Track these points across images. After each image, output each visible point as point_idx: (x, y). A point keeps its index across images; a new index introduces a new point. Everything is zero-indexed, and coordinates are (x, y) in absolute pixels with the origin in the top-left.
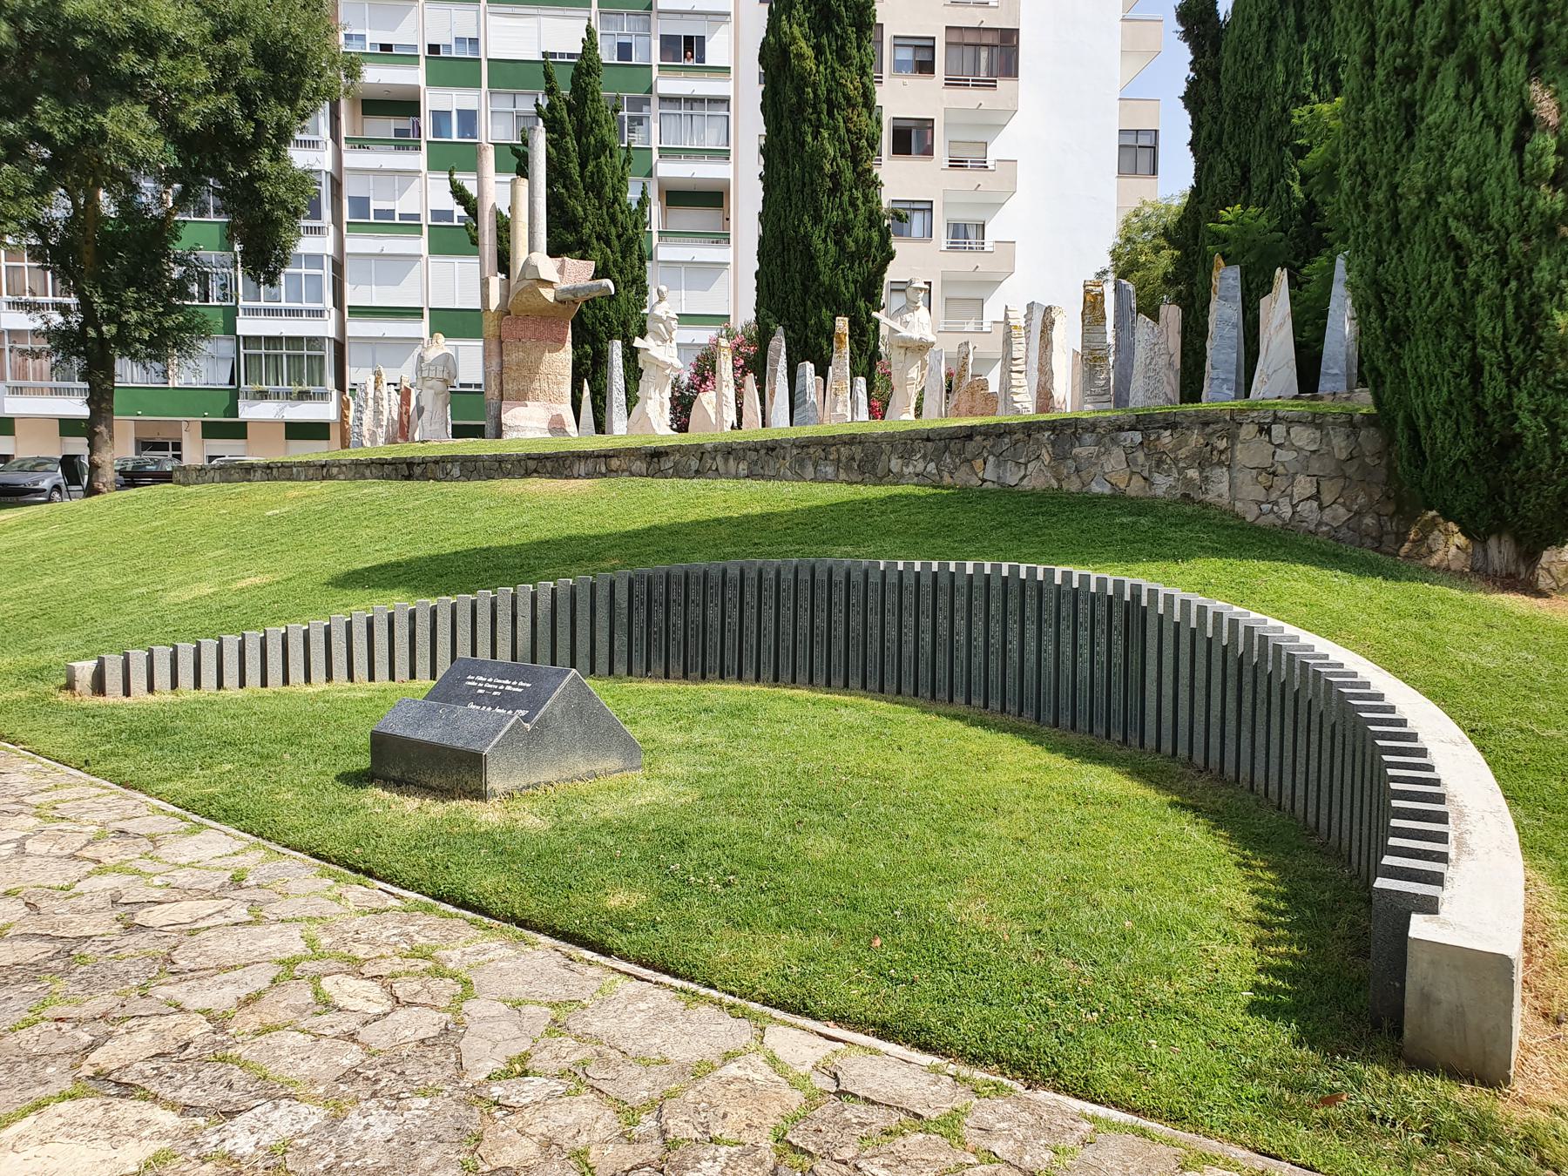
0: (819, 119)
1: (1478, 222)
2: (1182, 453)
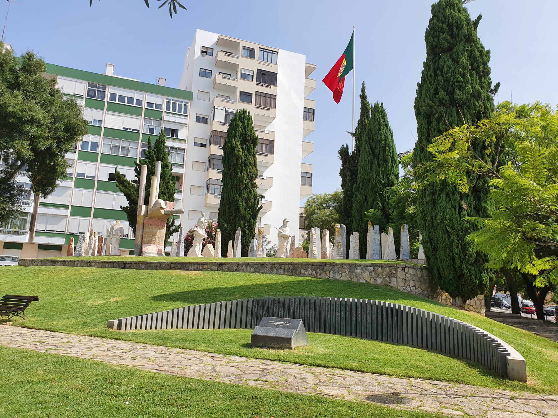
0: (242, 168)
1: (452, 227)
2: (384, 273)
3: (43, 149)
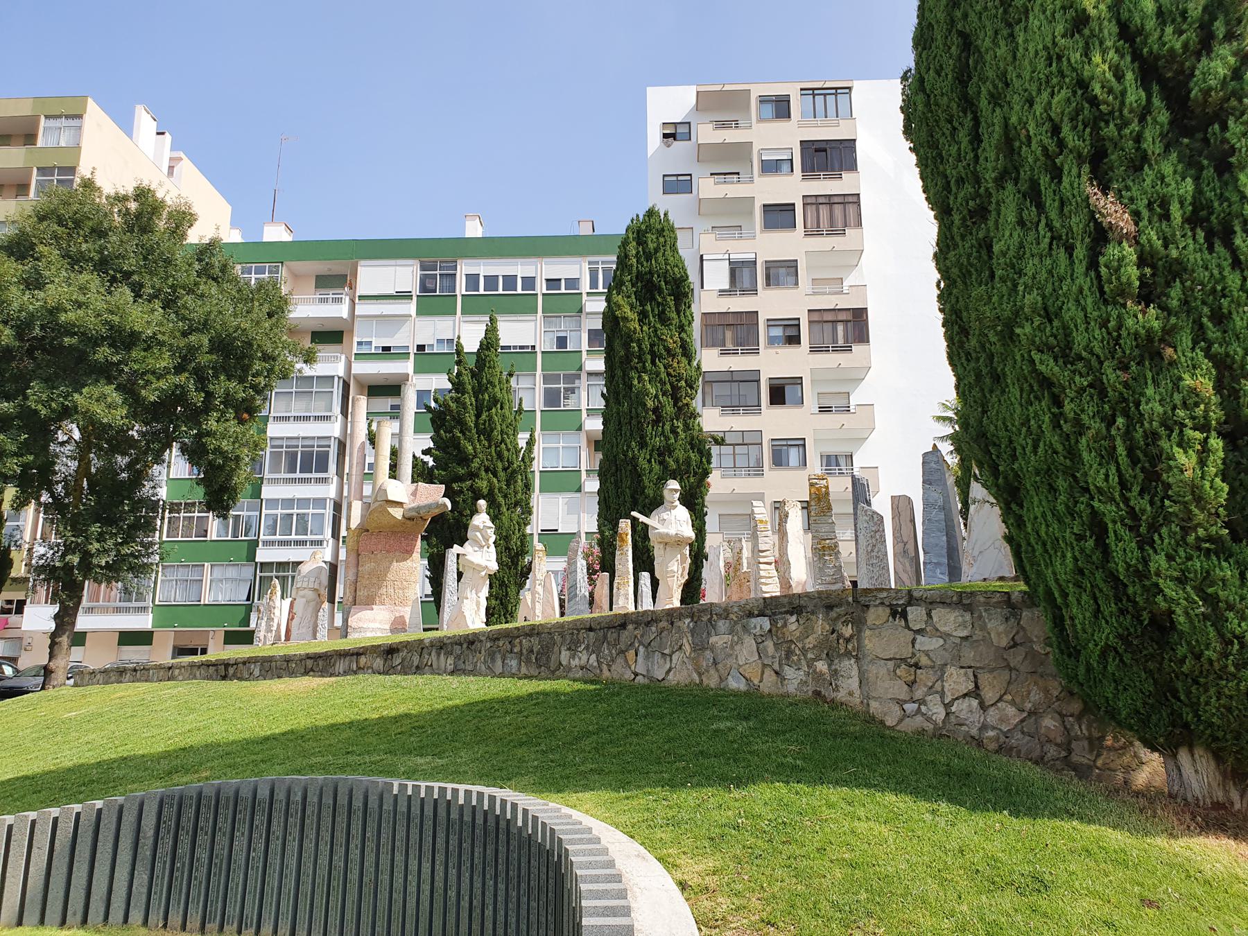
0: (644, 367)
1: (1065, 354)
3: (152, 398)
